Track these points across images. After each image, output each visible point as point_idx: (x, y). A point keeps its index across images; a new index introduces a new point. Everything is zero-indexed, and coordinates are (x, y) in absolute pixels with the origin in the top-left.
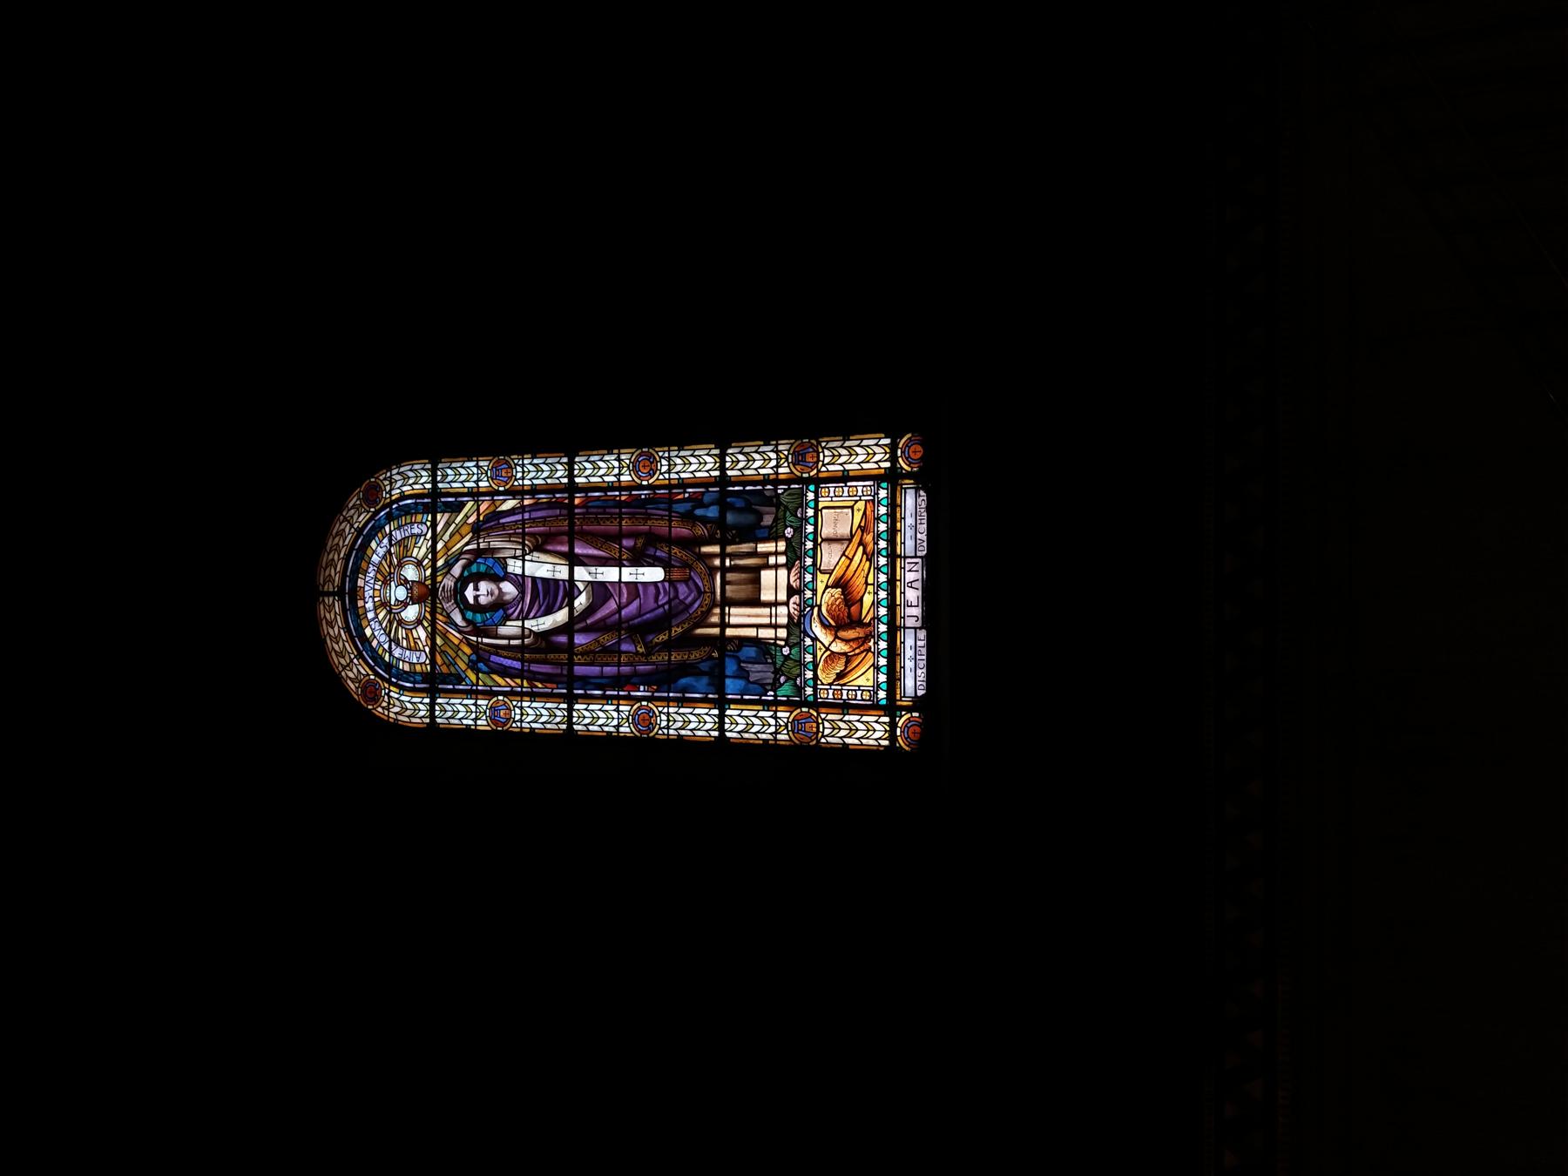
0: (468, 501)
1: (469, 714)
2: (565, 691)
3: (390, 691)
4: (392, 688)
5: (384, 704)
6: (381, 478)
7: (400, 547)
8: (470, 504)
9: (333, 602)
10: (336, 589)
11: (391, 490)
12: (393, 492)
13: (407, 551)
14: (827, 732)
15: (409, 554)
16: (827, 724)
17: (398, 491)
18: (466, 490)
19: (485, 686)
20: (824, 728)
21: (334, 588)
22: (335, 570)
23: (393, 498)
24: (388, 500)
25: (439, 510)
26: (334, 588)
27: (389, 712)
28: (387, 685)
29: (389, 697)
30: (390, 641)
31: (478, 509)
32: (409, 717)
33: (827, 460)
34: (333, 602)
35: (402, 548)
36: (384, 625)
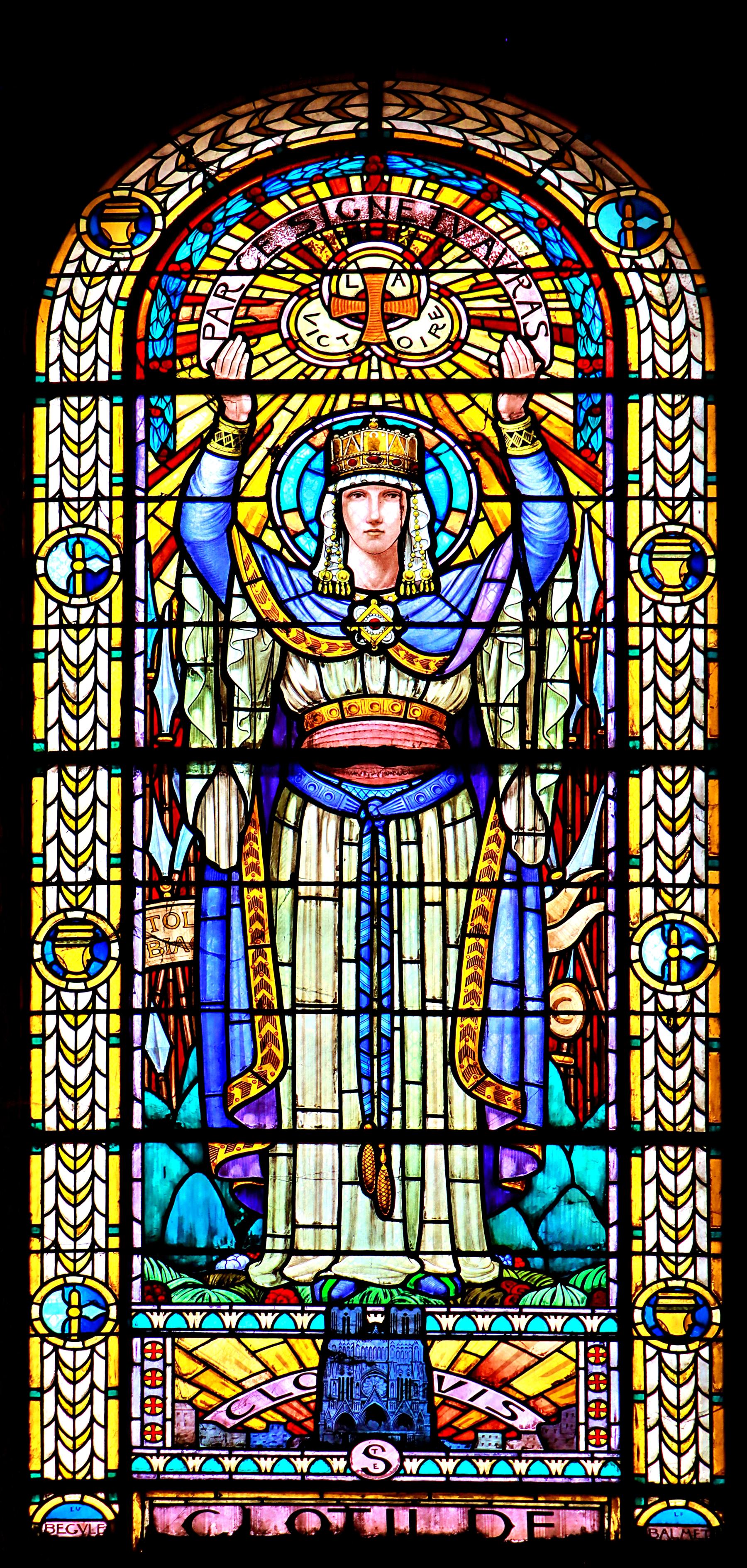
3: (125, 274)
4: (130, 280)
5: (91, 260)
6: (673, 247)
9: (353, 118)
10: (386, 125)
11: (641, 270)
12: (634, 277)
17: (638, 293)
18: (633, 463)
23: (619, 277)
24: (613, 262)
26: (387, 120)
27: (72, 276)
28: (138, 265)
29: (108, 274)
32: (62, 327)
34: (353, 118)
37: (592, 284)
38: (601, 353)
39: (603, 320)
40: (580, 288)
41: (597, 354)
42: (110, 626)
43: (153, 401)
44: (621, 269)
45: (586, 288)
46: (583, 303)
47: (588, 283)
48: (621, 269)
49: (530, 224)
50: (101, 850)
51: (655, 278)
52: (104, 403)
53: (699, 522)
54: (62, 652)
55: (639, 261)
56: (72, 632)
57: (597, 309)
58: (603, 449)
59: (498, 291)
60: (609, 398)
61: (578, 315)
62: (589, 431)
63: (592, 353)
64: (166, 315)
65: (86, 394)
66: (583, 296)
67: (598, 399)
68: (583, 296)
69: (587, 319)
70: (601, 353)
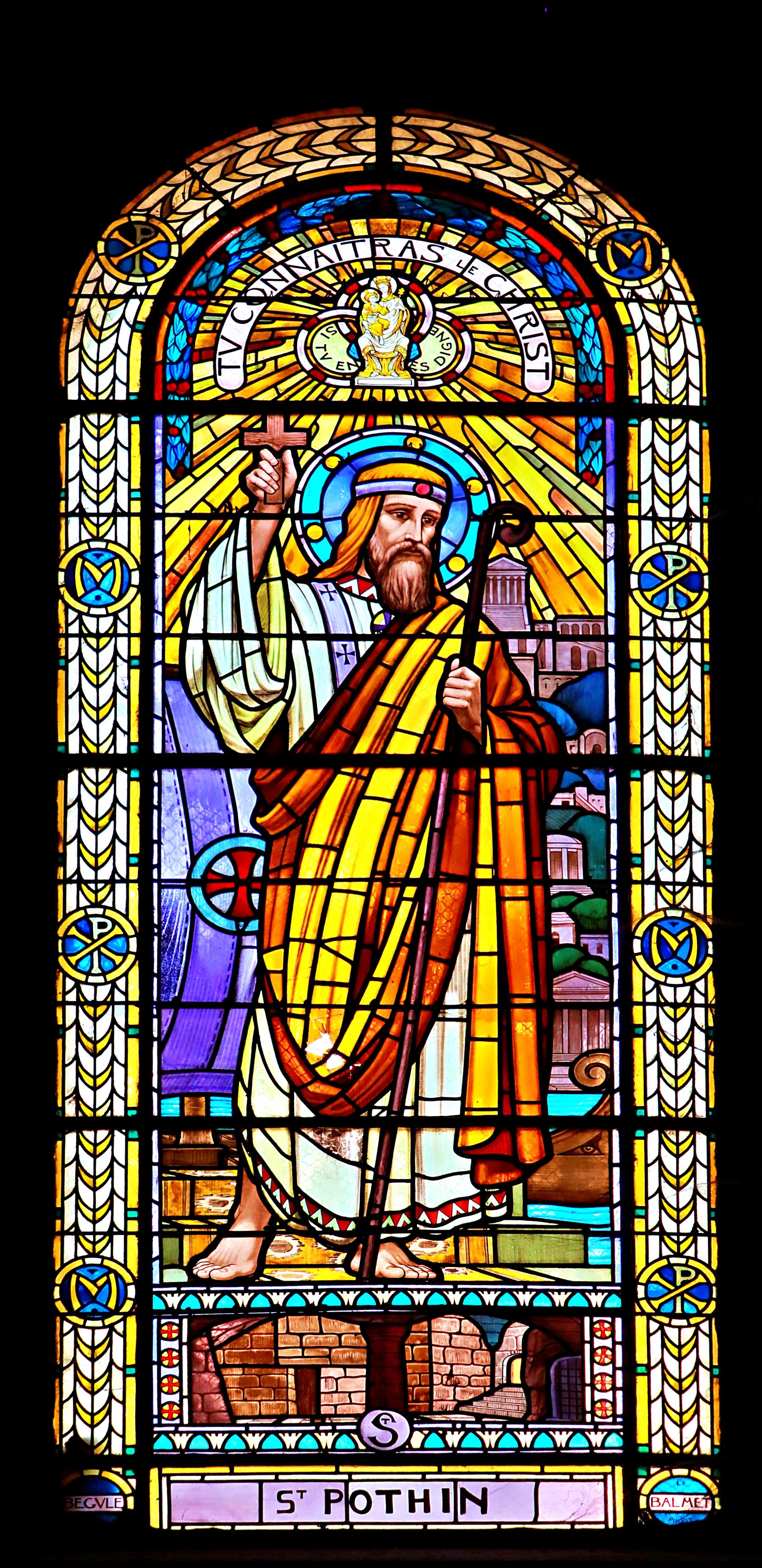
0: (604, 495)
1: (93, 495)
2: (158, 749)
7: (498, 324)
8: (599, 501)
13: (487, 342)
14: (86, 1335)
15: (481, 347)
16: (101, 1335)
19: (165, 537)
20: (93, 1329)
21: (398, 153)
22: (443, 157)
25: (583, 421)
30: (269, 300)
31: (585, 518)
33: (672, 1333)
35: (494, 328)
36: (303, 284)
37: (592, 314)
38: (601, 380)
39: (602, 349)
40: (581, 318)
41: (597, 381)
42: (129, 635)
43: (171, 420)
44: (622, 299)
45: (586, 318)
46: (583, 332)
47: (587, 312)
48: (622, 299)
49: (532, 258)
50: (120, 849)
51: (653, 307)
52: (122, 421)
53: (696, 545)
54: (82, 660)
55: (638, 291)
56: (93, 641)
57: (597, 339)
58: (603, 472)
59: (502, 318)
60: (609, 422)
61: (578, 343)
62: (591, 454)
63: (592, 380)
64: (182, 340)
65: (106, 412)
66: (583, 325)
67: (598, 423)
68: (583, 325)
69: (587, 346)
70: (601, 380)
